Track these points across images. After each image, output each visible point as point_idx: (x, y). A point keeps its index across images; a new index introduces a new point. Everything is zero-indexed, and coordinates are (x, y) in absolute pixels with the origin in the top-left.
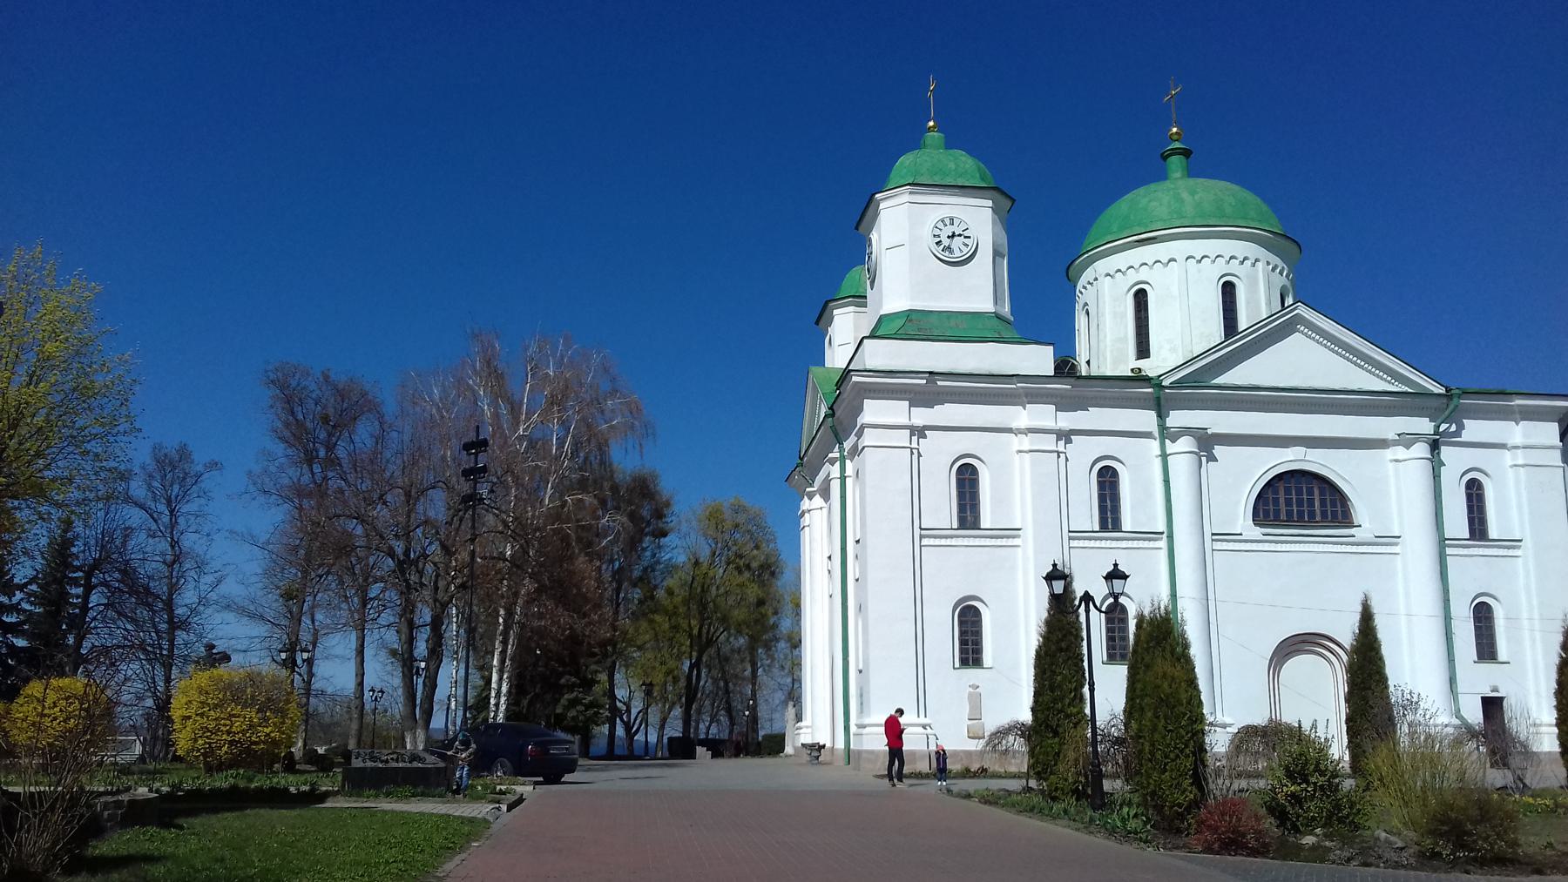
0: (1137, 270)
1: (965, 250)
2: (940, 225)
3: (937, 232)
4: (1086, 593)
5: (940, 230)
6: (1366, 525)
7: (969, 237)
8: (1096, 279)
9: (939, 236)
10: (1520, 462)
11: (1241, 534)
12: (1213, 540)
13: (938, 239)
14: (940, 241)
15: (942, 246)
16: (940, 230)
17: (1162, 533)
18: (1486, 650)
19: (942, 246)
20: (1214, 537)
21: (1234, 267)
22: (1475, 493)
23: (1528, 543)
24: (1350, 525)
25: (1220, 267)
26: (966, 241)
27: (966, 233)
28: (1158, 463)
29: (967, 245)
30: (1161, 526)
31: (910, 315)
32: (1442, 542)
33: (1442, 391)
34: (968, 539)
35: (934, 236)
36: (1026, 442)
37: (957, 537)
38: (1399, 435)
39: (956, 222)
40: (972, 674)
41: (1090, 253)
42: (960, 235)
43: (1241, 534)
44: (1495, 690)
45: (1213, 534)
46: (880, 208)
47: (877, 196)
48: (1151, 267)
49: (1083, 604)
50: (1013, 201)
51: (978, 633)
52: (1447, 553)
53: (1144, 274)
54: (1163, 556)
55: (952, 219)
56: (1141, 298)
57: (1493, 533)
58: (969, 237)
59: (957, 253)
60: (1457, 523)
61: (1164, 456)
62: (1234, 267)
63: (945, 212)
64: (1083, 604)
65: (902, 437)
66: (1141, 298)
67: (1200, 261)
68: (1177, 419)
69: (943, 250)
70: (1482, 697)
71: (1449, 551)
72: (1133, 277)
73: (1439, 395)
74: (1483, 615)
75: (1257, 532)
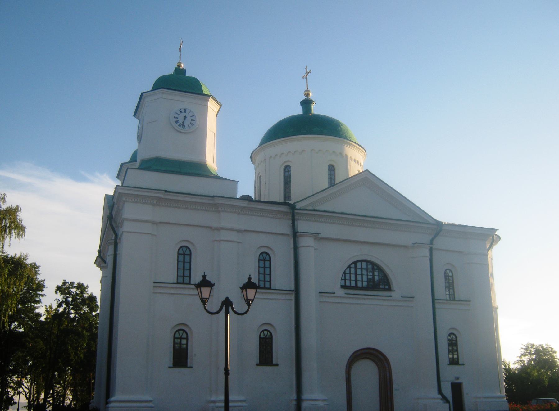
2: (179, 112)
3: (176, 115)
4: (227, 299)
5: (178, 114)
7: (195, 120)
8: (265, 159)
9: (177, 118)
11: (334, 293)
13: (177, 120)
14: (178, 121)
16: (178, 114)
19: (178, 124)
24: (390, 289)
29: (193, 125)
35: (175, 117)
37: (176, 288)
38: (414, 244)
39: (188, 112)
43: (334, 293)
44: (458, 378)
47: (144, 94)
49: (224, 307)
50: (221, 105)
61: (296, 249)
64: (224, 307)
69: (179, 126)
71: (437, 306)
75: (342, 292)
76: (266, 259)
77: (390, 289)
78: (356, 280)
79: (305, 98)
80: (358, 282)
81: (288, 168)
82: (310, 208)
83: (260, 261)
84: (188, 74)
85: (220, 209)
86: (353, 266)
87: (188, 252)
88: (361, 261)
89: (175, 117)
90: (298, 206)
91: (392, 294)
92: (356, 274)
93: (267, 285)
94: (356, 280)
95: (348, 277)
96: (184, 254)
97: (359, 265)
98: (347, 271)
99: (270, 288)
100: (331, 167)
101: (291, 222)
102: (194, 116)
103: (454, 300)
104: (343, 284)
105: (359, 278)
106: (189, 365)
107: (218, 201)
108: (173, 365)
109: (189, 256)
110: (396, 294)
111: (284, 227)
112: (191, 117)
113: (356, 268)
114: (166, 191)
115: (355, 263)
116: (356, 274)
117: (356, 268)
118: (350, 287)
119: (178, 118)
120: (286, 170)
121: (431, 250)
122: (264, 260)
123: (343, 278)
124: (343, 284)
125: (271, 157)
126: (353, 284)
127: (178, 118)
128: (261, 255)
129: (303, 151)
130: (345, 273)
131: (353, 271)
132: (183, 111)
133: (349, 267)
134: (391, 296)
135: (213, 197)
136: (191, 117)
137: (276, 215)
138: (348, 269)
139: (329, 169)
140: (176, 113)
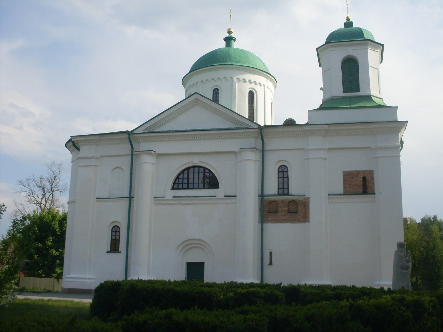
86: (186, 172)
88: (194, 167)
92: (188, 178)
97: (191, 170)
113: (188, 173)
115: (188, 169)
116: (188, 178)
131: (186, 176)
133: (182, 172)
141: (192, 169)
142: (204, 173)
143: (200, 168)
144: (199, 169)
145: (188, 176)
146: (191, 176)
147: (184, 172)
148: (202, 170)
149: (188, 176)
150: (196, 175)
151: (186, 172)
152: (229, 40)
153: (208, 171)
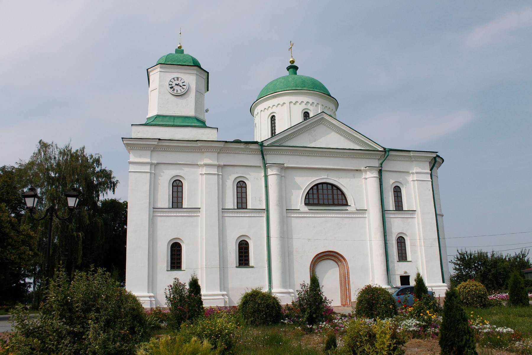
0: (272, 108)
1: (183, 90)
2: (173, 80)
3: (171, 83)
6: (353, 205)
7: (185, 85)
8: (258, 113)
9: (172, 85)
10: (415, 179)
11: (299, 210)
12: (286, 212)
13: (171, 86)
15: (172, 89)
17: (264, 209)
18: (403, 257)
20: (288, 211)
21: (309, 106)
22: (397, 191)
23: (419, 212)
25: (303, 106)
26: (184, 87)
27: (184, 84)
28: (263, 179)
30: (264, 207)
31: (158, 116)
32: (383, 211)
33: (382, 149)
34: (177, 213)
35: (170, 85)
36: (204, 170)
39: (180, 79)
40: (176, 274)
41: (256, 103)
42: (181, 86)
44: (406, 273)
45: (286, 210)
46: (150, 75)
47: (149, 70)
48: (277, 106)
51: (180, 255)
52: (386, 216)
53: (274, 109)
54: (265, 219)
55: (178, 78)
56: (273, 118)
57: (405, 208)
58: (185, 85)
59: (179, 92)
60: (390, 204)
61: (266, 177)
62: (309, 106)
63: (175, 75)
65: (147, 169)
66: (273, 118)
67: (295, 104)
68: (270, 159)
69: (173, 91)
70: (400, 276)
71: (386, 216)
72: (271, 111)
73: (381, 151)
74: (401, 241)
75: (306, 209)
76: (243, 186)
77: (347, 205)
78: (318, 199)
79: (290, 64)
80: (320, 200)
81: (274, 117)
82: (278, 145)
83: (238, 188)
84: (185, 53)
85: (203, 150)
86: (315, 187)
87: (180, 184)
88: (322, 184)
89: (170, 85)
90: (266, 144)
91: (348, 208)
92: (318, 194)
93: (244, 206)
94: (318, 199)
95: (311, 196)
96: (178, 186)
97: (320, 186)
98: (311, 192)
99: (246, 208)
100: (306, 113)
101: (261, 156)
102: (184, 82)
103: (402, 210)
104: (307, 202)
105: (321, 197)
106: (183, 269)
107: (199, 144)
108: (171, 269)
109: (181, 187)
110: (352, 208)
111: (256, 160)
112: (182, 83)
113: (318, 189)
114: (159, 139)
115: (317, 185)
116: (318, 194)
117: (318, 189)
118: (314, 204)
119: (172, 85)
120: (273, 119)
121: (380, 172)
122: (241, 187)
123: (307, 197)
124: (307, 202)
125: (262, 111)
126: (316, 201)
127: (172, 85)
128: (239, 183)
129: (284, 103)
130: (308, 193)
131: (315, 191)
132: (176, 79)
133: (312, 188)
134: (347, 210)
135: (197, 141)
136: (182, 83)
137: (247, 152)
138: (311, 190)
139: (305, 115)
140: (171, 81)
141: (321, 185)
142: (332, 189)
143: (324, 185)
144: (327, 186)
145: (318, 191)
146: (320, 191)
147: (314, 188)
148: (330, 187)
149: (318, 191)
150: (325, 191)
151: (315, 187)
152: (293, 68)
153: (336, 189)
